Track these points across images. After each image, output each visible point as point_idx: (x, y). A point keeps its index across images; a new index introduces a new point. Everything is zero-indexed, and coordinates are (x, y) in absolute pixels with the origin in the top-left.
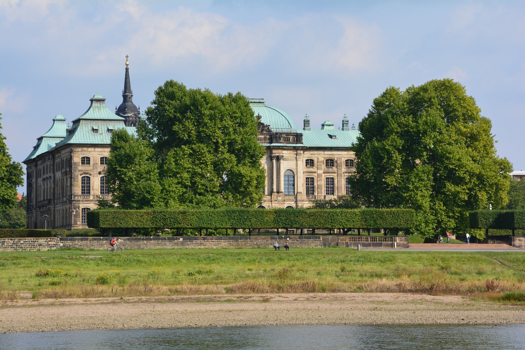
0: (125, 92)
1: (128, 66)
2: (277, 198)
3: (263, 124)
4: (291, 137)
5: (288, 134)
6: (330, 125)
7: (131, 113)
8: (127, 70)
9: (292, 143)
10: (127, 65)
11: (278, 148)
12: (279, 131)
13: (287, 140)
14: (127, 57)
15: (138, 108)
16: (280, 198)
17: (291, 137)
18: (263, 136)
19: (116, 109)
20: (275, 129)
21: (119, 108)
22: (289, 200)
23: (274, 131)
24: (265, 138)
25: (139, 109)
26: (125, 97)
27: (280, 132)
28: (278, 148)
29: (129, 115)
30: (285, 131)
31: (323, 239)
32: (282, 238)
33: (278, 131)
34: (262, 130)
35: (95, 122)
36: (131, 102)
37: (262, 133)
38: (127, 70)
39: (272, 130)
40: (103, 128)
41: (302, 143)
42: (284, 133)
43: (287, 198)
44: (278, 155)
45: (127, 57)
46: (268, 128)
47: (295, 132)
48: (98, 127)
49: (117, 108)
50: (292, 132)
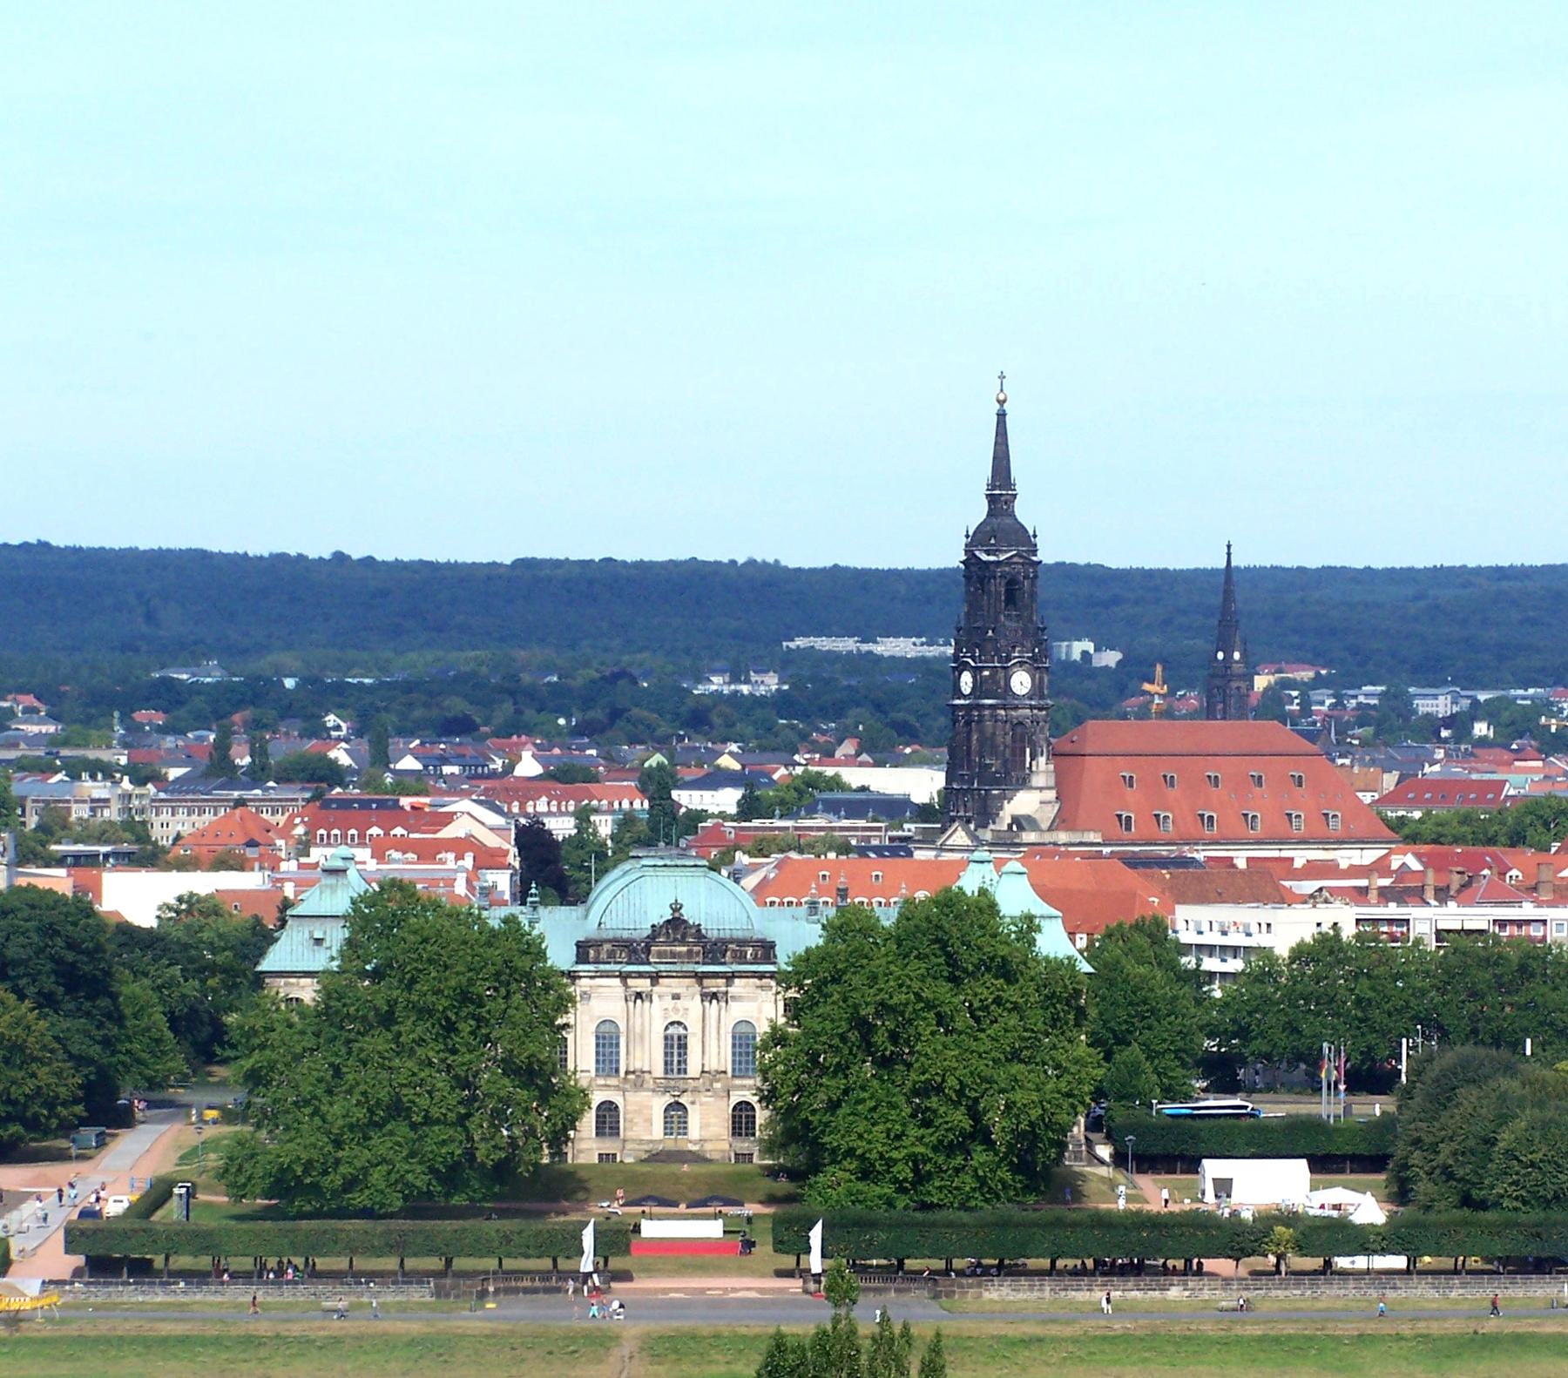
0: (992, 486)
1: (1006, 406)
2: (711, 1085)
3: (685, 922)
4: (750, 951)
5: (743, 943)
6: (982, 862)
7: (1006, 552)
8: (1001, 416)
9: (752, 963)
10: (1002, 402)
11: (715, 975)
12: (727, 935)
13: (741, 958)
14: (1002, 377)
15: (1031, 533)
16: (717, 1085)
17: (750, 951)
18: (684, 949)
19: (967, 536)
20: (715, 932)
21: (975, 533)
22: (743, 1087)
23: (713, 935)
24: (690, 952)
25: (1035, 536)
26: (992, 499)
27: (728, 936)
28: (715, 975)
29: (1002, 558)
30: (739, 935)
31: (436, 1286)
32: (361, 1283)
33: (722, 935)
34: (684, 936)
35: (318, 922)
36: (1012, 515)
37: (683, 942)
38: (1001, 416)
39: (709, 935)
40: (334, 935)
41: (774, 963)
42: (732, 941)
43: (738, 1082)
44: (714, 990)
45: (1002, 377)
46: (699, 931)
47: (760, 937)
48: (325, 933)
49: (971, 533)
50: (755, 937)
